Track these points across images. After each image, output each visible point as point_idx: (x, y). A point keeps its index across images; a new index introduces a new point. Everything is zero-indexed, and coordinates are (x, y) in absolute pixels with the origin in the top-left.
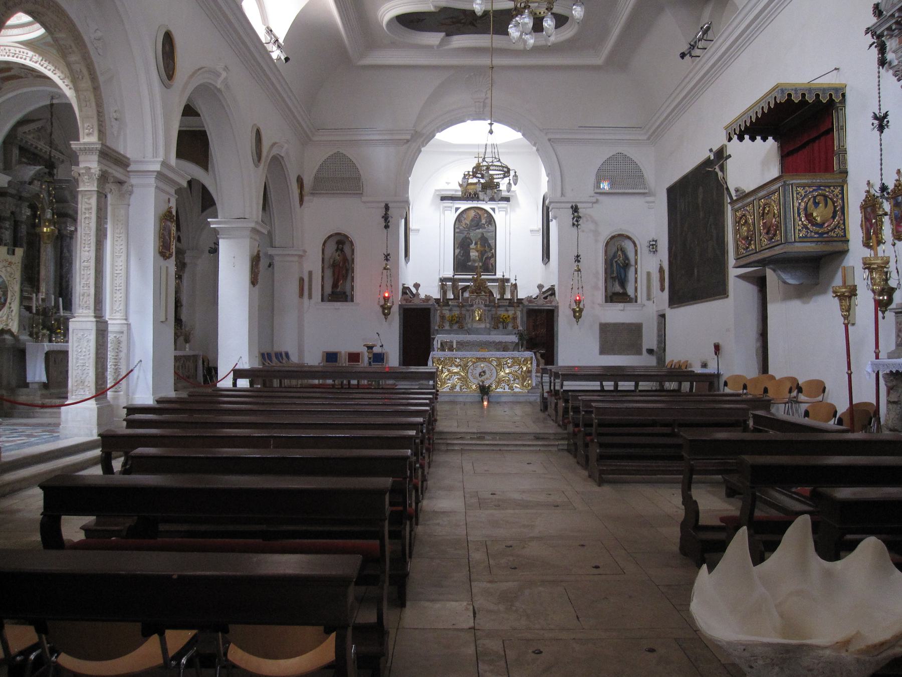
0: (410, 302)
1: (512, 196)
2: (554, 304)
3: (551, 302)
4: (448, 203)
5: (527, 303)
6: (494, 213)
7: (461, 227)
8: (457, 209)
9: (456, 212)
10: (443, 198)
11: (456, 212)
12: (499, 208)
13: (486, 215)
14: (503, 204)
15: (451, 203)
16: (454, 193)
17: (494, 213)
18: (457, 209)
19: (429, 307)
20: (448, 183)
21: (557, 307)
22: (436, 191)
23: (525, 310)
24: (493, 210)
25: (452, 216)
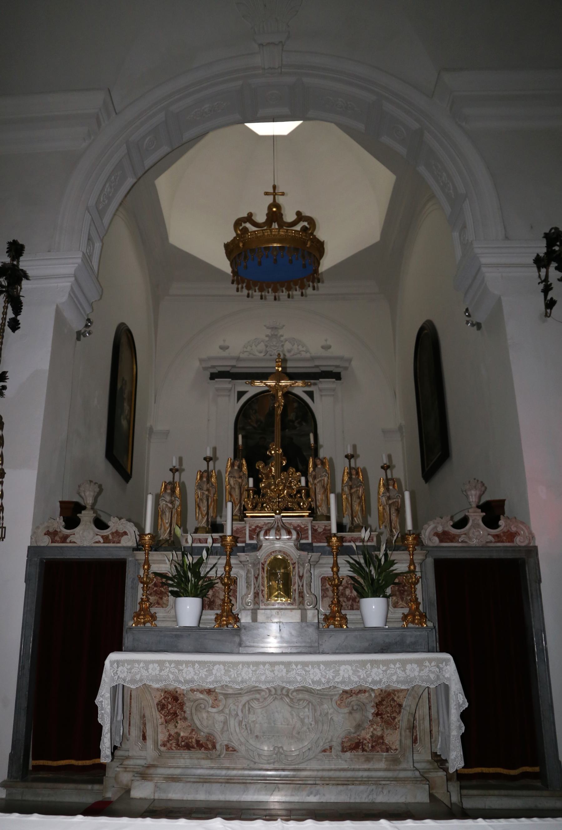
0: (64, 539)
1: (346, 368)
2: (519, 541)
3: (511, 536)
4: (225, 383)
5: (436, 540)
6: (313, 400)
7: (248, 427)
8: (241, 394)
9: (239, 399)
10: (213, 376)
11: (239, 399)
12: (320, 390)
13: (296, 405)
14: (326, 384)
15: (230, 382)
16: (233, 363)
17: (313, 400)
18: (241, 394)
19: (121, 555)
20: (224, 348)
21: (532, 551)
22: (201, 361)
23: (430, 561)
24: (311, 394)
25: (234, 407)
